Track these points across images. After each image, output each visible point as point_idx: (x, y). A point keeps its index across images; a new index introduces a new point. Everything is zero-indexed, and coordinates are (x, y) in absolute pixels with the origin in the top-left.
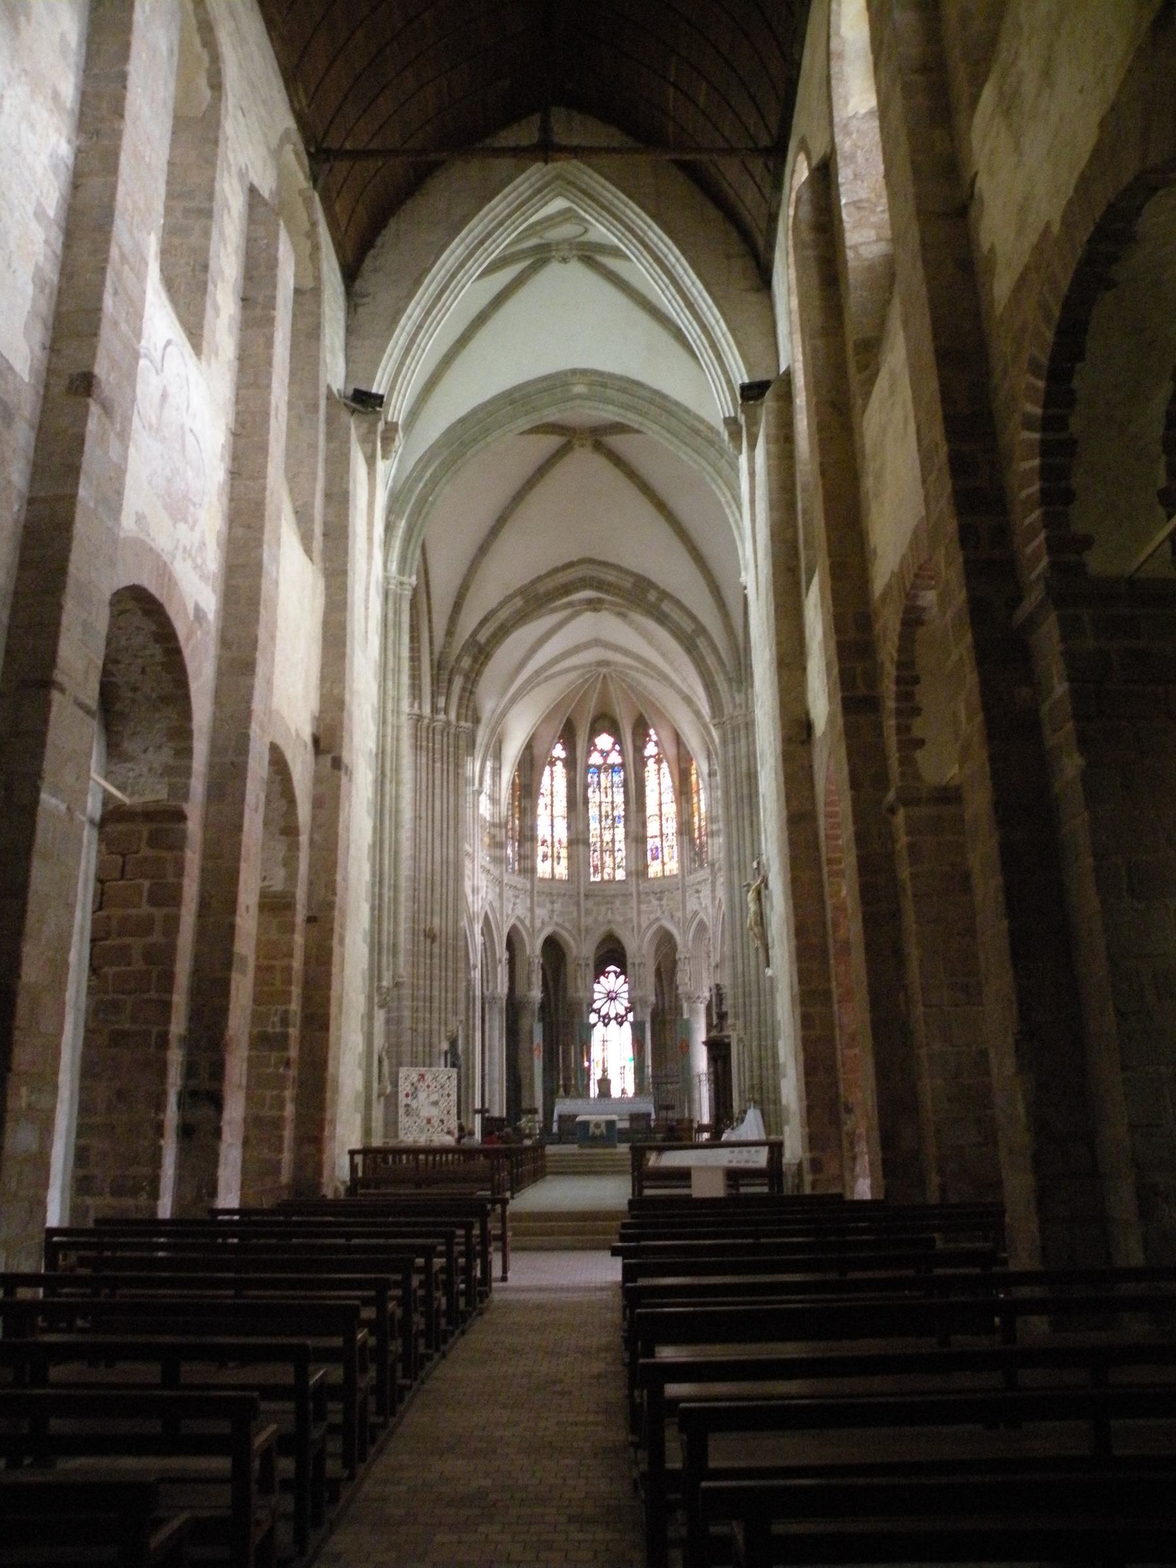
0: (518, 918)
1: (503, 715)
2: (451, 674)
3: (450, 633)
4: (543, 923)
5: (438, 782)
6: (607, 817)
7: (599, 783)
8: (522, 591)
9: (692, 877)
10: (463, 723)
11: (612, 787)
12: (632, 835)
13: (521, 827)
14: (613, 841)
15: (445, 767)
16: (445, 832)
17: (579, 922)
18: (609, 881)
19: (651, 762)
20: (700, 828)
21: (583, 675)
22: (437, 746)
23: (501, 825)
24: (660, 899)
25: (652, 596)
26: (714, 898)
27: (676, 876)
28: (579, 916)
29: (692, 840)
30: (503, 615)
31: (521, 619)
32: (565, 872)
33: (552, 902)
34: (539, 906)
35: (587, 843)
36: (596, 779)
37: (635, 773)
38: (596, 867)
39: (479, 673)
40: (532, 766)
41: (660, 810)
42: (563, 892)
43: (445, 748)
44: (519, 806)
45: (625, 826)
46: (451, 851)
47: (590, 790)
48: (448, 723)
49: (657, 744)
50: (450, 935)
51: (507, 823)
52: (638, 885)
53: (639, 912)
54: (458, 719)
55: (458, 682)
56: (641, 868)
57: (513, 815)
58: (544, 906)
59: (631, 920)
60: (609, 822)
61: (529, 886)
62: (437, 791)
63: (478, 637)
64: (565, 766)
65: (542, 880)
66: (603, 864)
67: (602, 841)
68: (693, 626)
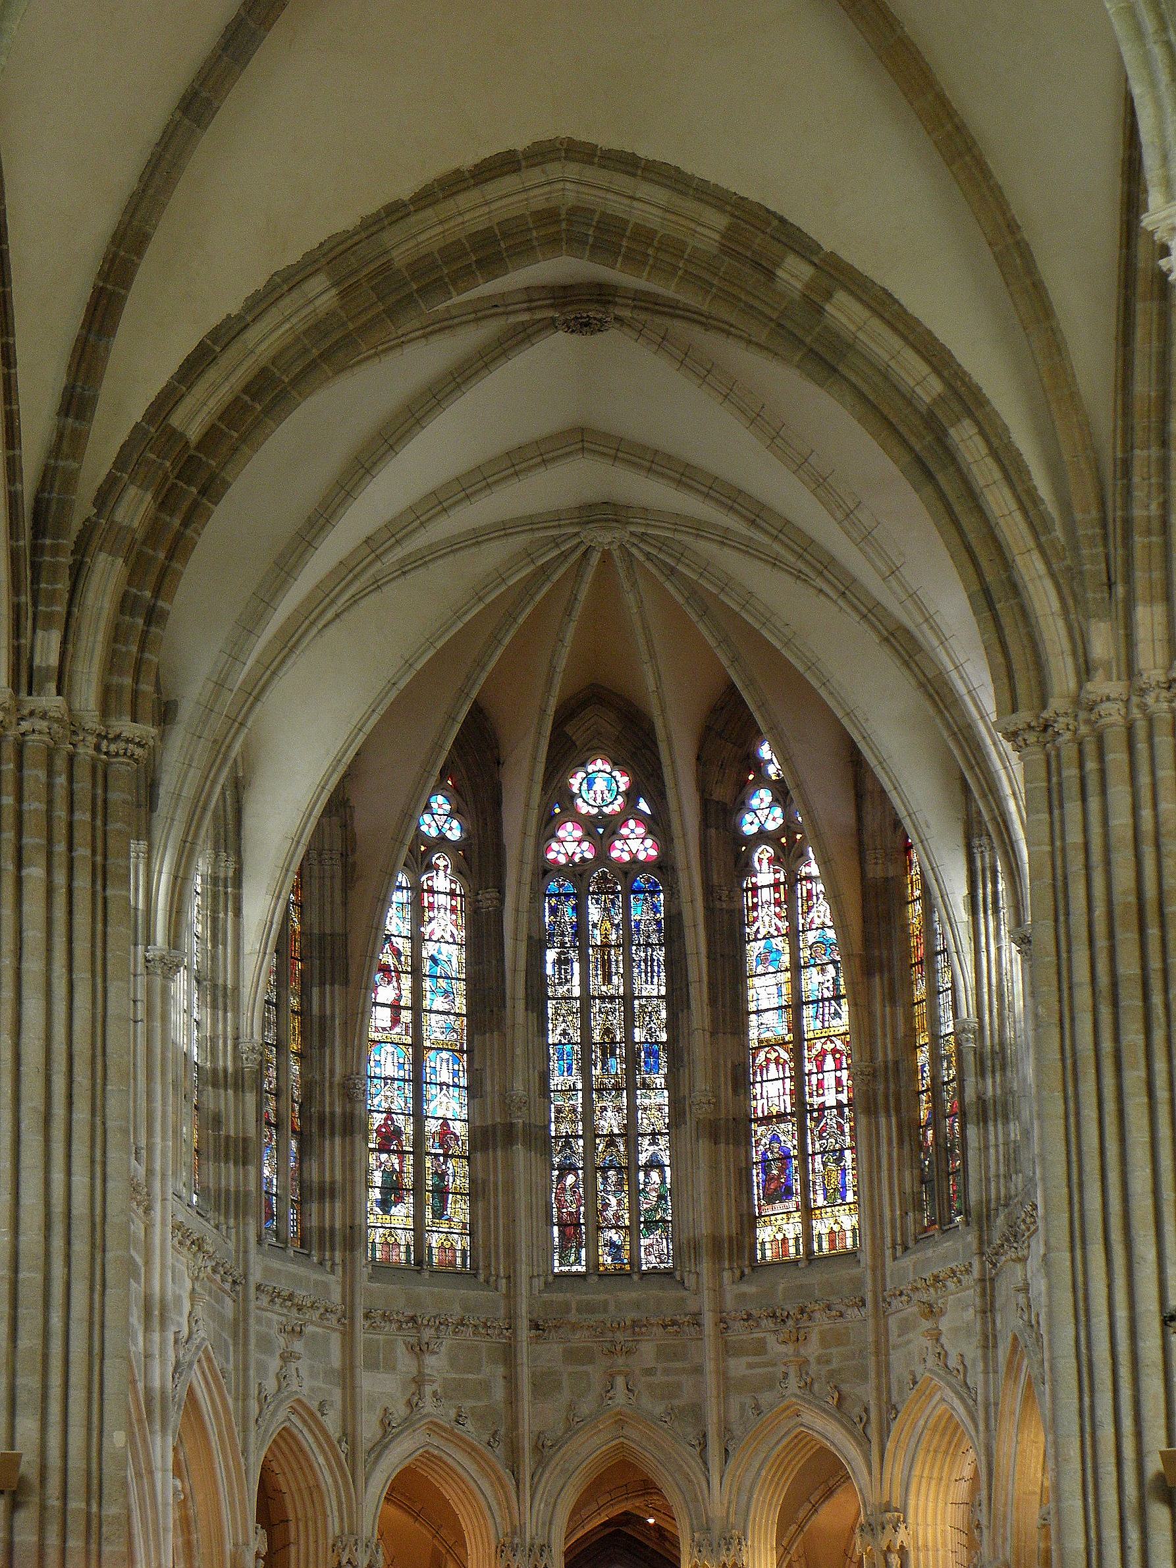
0: (300, 1408)
1: (255, 692)
2: (82, 546)
4: (386, 1424)
5: (34, 934)
6: (608, 1049)
7: (581, 929)
9: (908, 1262)
10: (124, 726)
11: (626, 943)
12: (699, 1111)
13: (308, 1087)
14: (631, 1133)
15: (60, 879)
16: (59, 1110)
17: (514, 1424)
18: (618, 1274)
19: (764, 852)
20: (936, 1087)
21: (527, 555)
22: (34, 806)
23: (237, 1081)
24: (798, 1338)
26: (989, 1342)
27: (852, 1255)
28: (513, 1398)
29: (909, 1130)
31: (325, 356)
32: (461, 1243)
33: (419, 1350)
34: (372, 1366)
35: (540, 1141)
36: (569, 915)
37: (709, 890)
38: (569, 1226)
39: (179, 548)
40: (349, 876)
41: (796, 1027)
42: (457, 1311)
43: (61, 813)
44: (303, 1013)
45: (672, 1084)
46: (80, 1180)
47: (551, 955)
48: (74, 726)
49: (781, 794)
50: (76, 1480)
51: (260, 1074)
52: (718, 1291)
53: (727, 1385)
56: (728, 1228)
57: (280, 1046)
58: (391, 1368)
59: (696, 1412)
60: (616, 1066)
61: (336, 1297)
63: (176, 420)
64: (459, 871)
65: (383, 1270)
66: (596, 1211)
67: (591, 1133)
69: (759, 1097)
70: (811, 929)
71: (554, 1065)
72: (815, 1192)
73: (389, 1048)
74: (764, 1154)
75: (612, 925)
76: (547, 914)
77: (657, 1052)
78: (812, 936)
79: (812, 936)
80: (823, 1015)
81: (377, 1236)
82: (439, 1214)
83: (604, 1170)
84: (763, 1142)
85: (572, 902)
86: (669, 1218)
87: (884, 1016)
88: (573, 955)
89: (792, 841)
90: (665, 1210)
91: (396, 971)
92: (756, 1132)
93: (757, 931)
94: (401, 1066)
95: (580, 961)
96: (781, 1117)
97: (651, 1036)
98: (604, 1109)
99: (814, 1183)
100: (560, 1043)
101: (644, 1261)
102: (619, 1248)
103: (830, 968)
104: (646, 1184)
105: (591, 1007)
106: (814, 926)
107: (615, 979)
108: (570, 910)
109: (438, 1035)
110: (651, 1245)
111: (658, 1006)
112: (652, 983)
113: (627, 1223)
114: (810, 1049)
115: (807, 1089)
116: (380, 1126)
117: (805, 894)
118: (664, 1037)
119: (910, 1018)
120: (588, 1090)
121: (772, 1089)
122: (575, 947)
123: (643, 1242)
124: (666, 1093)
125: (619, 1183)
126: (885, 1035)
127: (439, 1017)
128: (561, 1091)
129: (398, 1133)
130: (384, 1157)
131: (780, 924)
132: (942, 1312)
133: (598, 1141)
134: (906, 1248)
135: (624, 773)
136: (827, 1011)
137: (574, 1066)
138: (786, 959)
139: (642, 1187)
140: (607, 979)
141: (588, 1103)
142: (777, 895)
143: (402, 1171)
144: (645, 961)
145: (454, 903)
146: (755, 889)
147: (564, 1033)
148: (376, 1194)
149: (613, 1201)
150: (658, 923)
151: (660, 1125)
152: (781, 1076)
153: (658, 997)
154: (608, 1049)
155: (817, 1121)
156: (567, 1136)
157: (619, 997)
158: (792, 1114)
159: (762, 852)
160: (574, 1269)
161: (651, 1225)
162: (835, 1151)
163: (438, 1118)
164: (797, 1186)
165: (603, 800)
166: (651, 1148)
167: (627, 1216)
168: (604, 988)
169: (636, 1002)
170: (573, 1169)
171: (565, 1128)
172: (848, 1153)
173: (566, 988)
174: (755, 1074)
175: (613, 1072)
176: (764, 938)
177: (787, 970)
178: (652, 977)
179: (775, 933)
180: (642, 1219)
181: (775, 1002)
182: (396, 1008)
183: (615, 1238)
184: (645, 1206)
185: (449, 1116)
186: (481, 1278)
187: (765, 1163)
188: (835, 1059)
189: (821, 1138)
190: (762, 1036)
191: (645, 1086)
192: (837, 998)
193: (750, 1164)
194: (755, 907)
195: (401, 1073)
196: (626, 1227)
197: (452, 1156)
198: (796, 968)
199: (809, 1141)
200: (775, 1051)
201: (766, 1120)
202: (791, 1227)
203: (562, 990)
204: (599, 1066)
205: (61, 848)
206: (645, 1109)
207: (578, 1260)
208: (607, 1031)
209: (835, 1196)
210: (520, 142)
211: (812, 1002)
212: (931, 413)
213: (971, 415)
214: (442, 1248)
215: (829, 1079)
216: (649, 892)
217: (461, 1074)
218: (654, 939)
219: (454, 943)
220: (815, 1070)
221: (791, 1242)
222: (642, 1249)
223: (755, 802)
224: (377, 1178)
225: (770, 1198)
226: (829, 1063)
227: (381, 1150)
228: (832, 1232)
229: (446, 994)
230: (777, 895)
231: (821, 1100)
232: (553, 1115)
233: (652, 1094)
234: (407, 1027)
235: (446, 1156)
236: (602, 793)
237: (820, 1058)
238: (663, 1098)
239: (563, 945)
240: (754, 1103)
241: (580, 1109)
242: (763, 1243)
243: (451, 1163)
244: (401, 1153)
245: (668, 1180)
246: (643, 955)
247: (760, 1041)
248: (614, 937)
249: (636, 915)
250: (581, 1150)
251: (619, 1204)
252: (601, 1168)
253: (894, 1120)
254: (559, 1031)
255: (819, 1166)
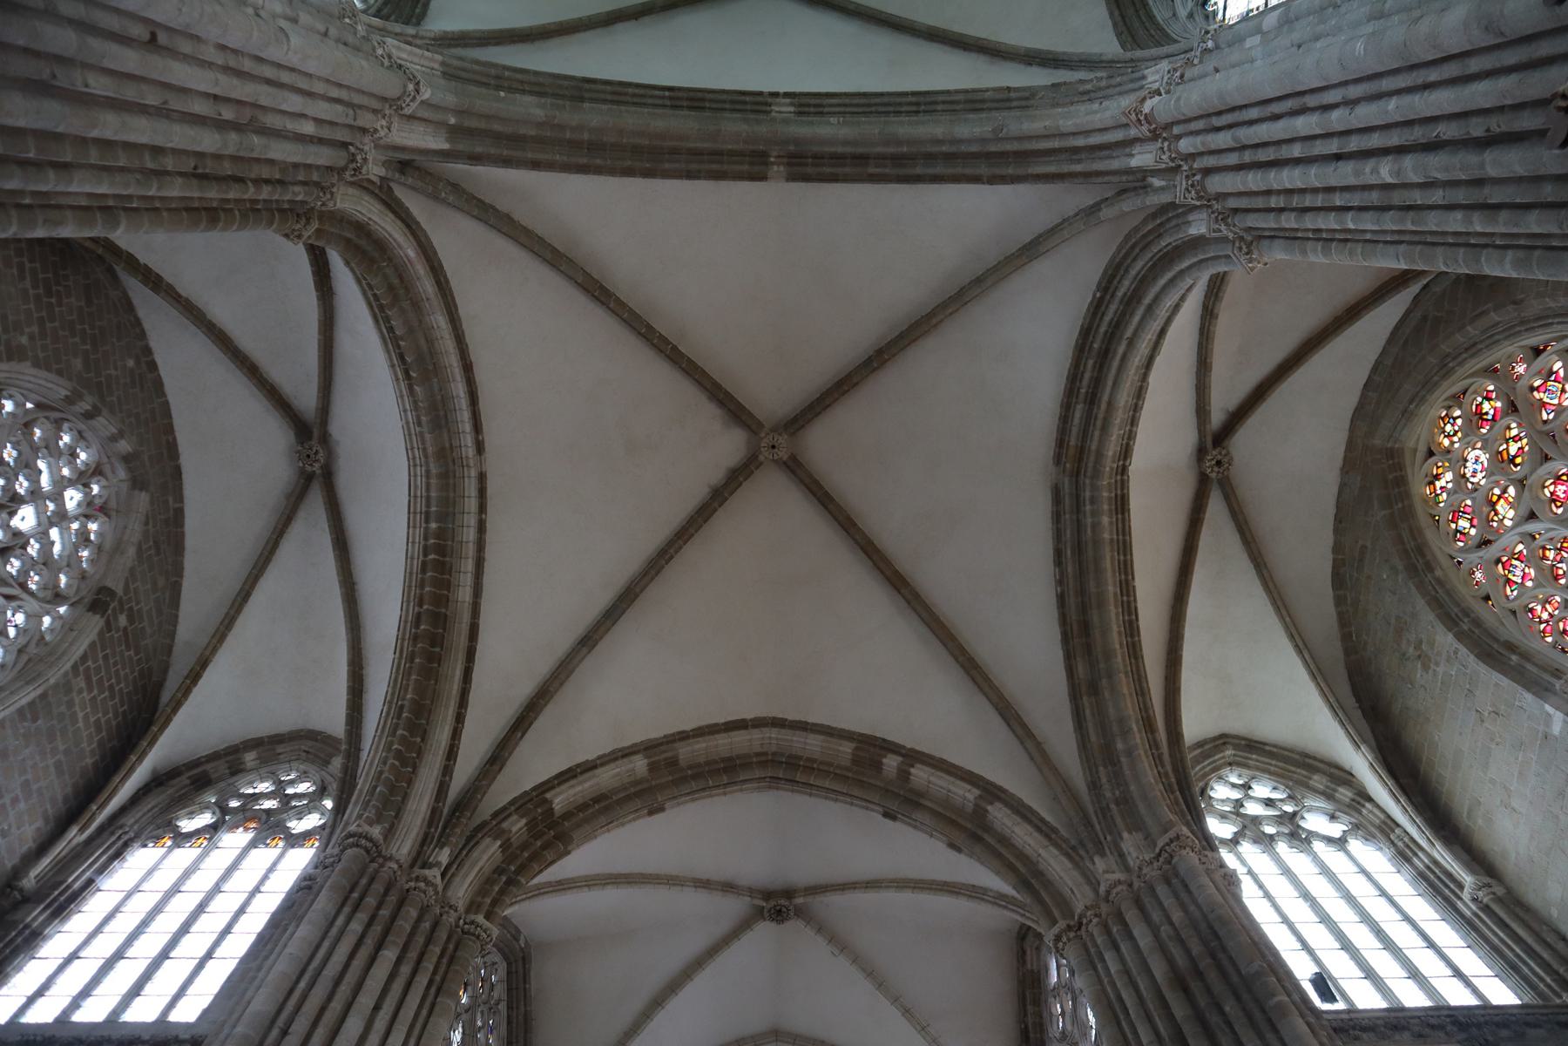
3: (497, 759)
8: (648, 748)
15: (406, 970)
25: (891, 763)
30: (606, 778)
43: (420, 940)
54: (473, 907)
55: (488, 853)
62: (366, 1000)
68: (977, 792)
205: (413, 955)
210: (749, 715)
212: (976, 805)
213: (999, 799)
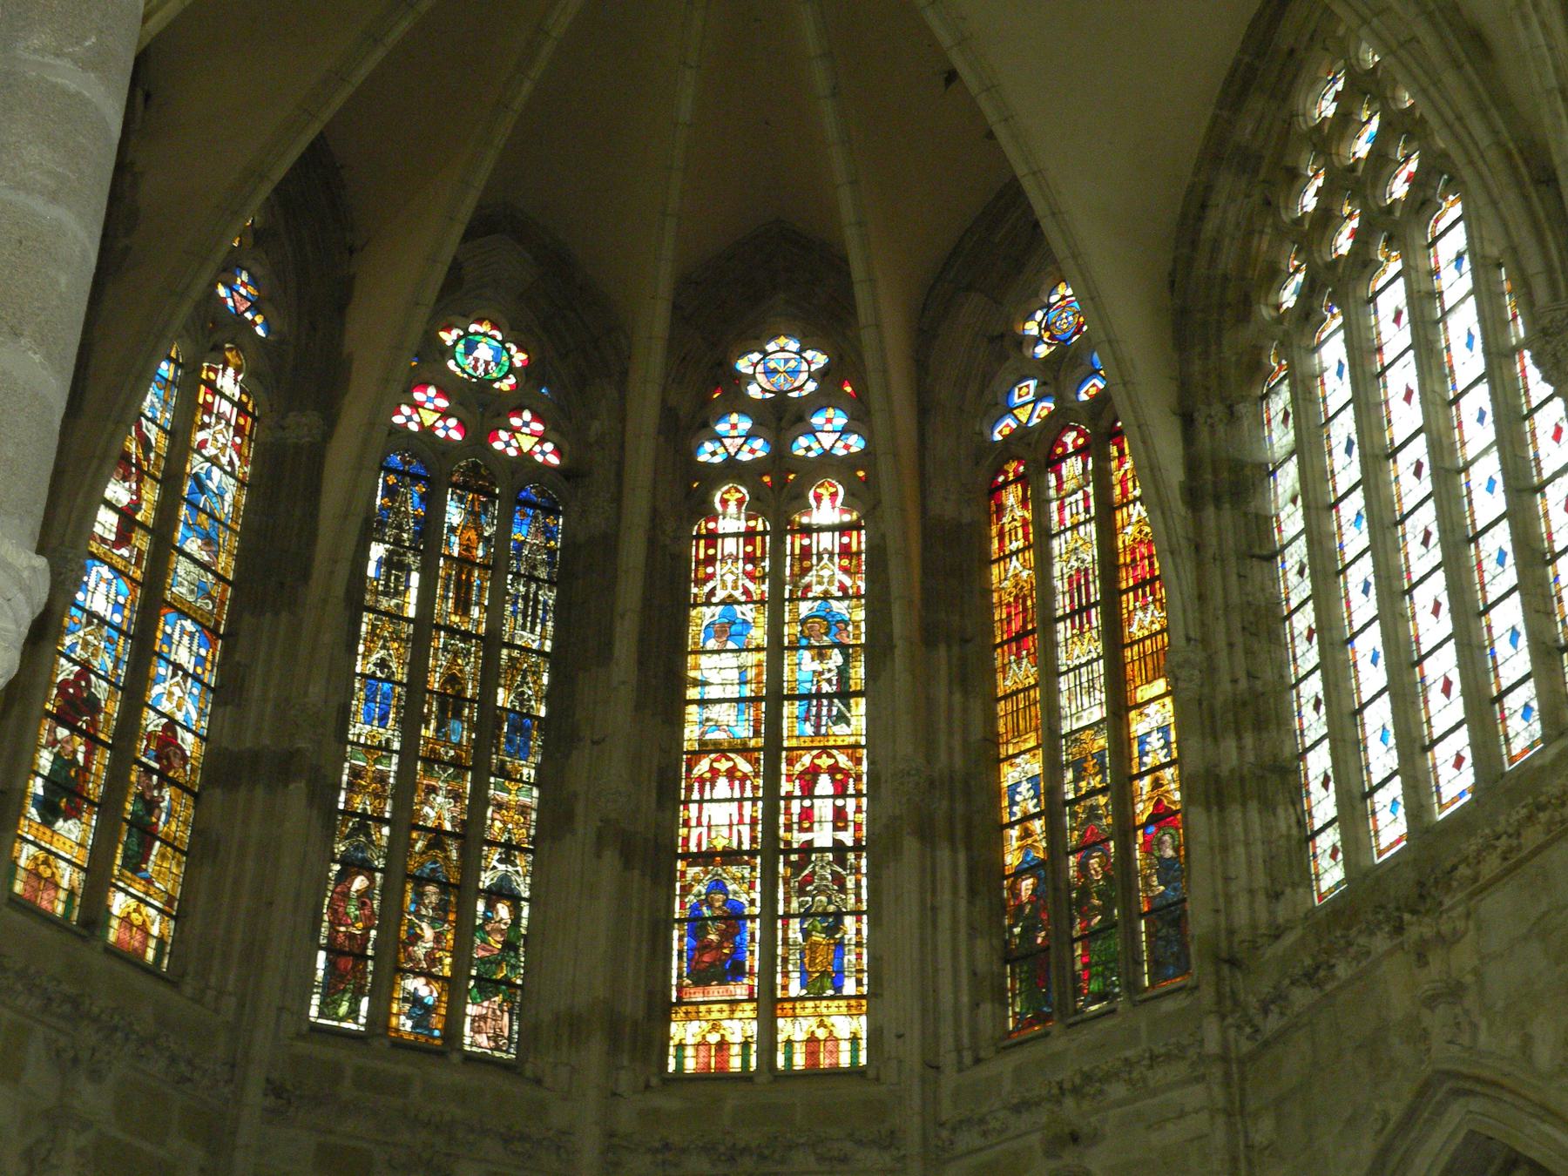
14: (470, 834)
36: (413, 505)
47: (377, 551)
60: (461, 733)
67: (406, 821)
69: (693, 822)
70: (804, 598)
71: (357, 704)
72: (786, 974)
73: (105, 572)
74: (695, 908)
75: (480, 536)
76: (380, 493)
77: (528, 729)
78: (804, 608)
79: (804, 608)
80: (818, 716)
81: (26, 855)
82: (135, 863)
83: (420, 882)
84: (696, 889)
85: (420, 488)
86: (519, 982)
87: (950, 709)
88: (410, 558)
89: (780, 483)
90: (514, 968)
91: (138, 466)
92: (683, 874)
93: (712, 592)
94: (118, 607)
95: (421, 570)
96: (731, 856)
97: (522, 705)
98: (433, 790)
99: (785, 960)
100: (373, 676)
101: (467, 1041)
102: (429, 1010)
103: (836, 658)
104: (487, 919)
105: (431, 639)
106: (810, 595)
107: (475, 612)
108: (416, 499)
109: (184, 590)
110: (483, 1018)
111: (537, 665)
112: (532, 631)
113: (447, 972)
114: (790, 762)
115: (782, 820)
116: (65, 683)
117: (797, 551)
118: (543, 712)
119: (992, 719)
120: (408, 754)
121: (720, 814)
122: (416, 549)
123: (471, 1010)
124: (535, 793)
125: (442, 907)
126: (951, 733)
127: (191, 567)
128: (364, 745)
129: (93, 706)
130: (62, 733)
131: (751, 586)
132: (1096, 1138)
133: (414, 835)
134: (977, 1061)
135: (521, 349)
136: (824, 711)
137: (392, 716)
138: (759, 635)
139: (479, 922)
140: (463, 607)
141: (405, 771)
142: (749, 549)
143: (87, 768)
144: (526, 598)
145: (242, 421)
146: (712, 538)
147: (382, 664)
148: (37, 787)
149: (428, 933)
150: (551, 552)
151: (520, 835)
152: (737, 794)
153: (540, 653)
154: (451, 703)
155: (797, 868)
156: (364, 816)
157: (477, 636)
158: (752, 853)
159: (728, 492)
160: (344, 1025)
161: (487, 986)
162: (825, 915)
163: (162, 715)
164: (753, 961)
165: (486, 372)
166: (502, 867)
167: (448, 961)
168: (455, 619)
169: (505, 652)
170: (367, 869)
171: (361, 803)
172: (849, 921)
173: (393, 602)
174: (689, 789)
175: (454, 739)
176: (722, 602)
177: (758, 649)
178: (534, 624)
179: (743, 598)
180: (474, 972)
181: (733, 692)
182: (127, 517)
183: (424, 991)
184: (482, 953)
185: (180, 717)
186: (188, 990)
187: (696, 924)
188: (834, 781)
189: (802, 892)
190: (708, 737)
191: (504, 773)
192: (845, 695)
193: (669, 922)
194: (710, 561)
195: (117, 619)
196: (444, 978)
197: (173, 783)
198: (776, 649)
199: (781, 896)
200: (729, 759)
201: (705, 858)
202: (736, 1024)
203: (386, 603)
204: (433, 725)
206: (500, 806)
207: (353, 1014)
208: (451, 679)
209: (823, 984)
211: (801, 697)
214: (126, 920)
215: (823, 809)
216: (544, 509)
217: (209, 666)
218: (542, 573)
219: (232, 475)
220: (797, 792)
221: (735, 1050)
222: (468, 1020)
223: (722, 428)
224: (45, 760)
225: (701, 978)
226: (824, 785)
227: (60, 719)
228: (812, 1040)
229: (208, 541)
230: (749, 549)
231: (806, 837)
232: (345, 778)
233: (512, 786)
234: (140, 554)
235: (165, 779)
236: (487, 363)
237: (807, 777)
238: (531, 798)
239: (398, 542)
240: (683, 831)
241: (391, 780)
242: (681, 1047)
243: (167, 793)
244: (92, 741)
245: (524, 922)
246: (522, 589)
247: (702, 743)
248: (480, 553)
249: (518, 535)
250: (384, 842)
251: (438, 938)
252: (413, 877)
253: (962, 858)
254: (374, 658)
255: (795, 933)
